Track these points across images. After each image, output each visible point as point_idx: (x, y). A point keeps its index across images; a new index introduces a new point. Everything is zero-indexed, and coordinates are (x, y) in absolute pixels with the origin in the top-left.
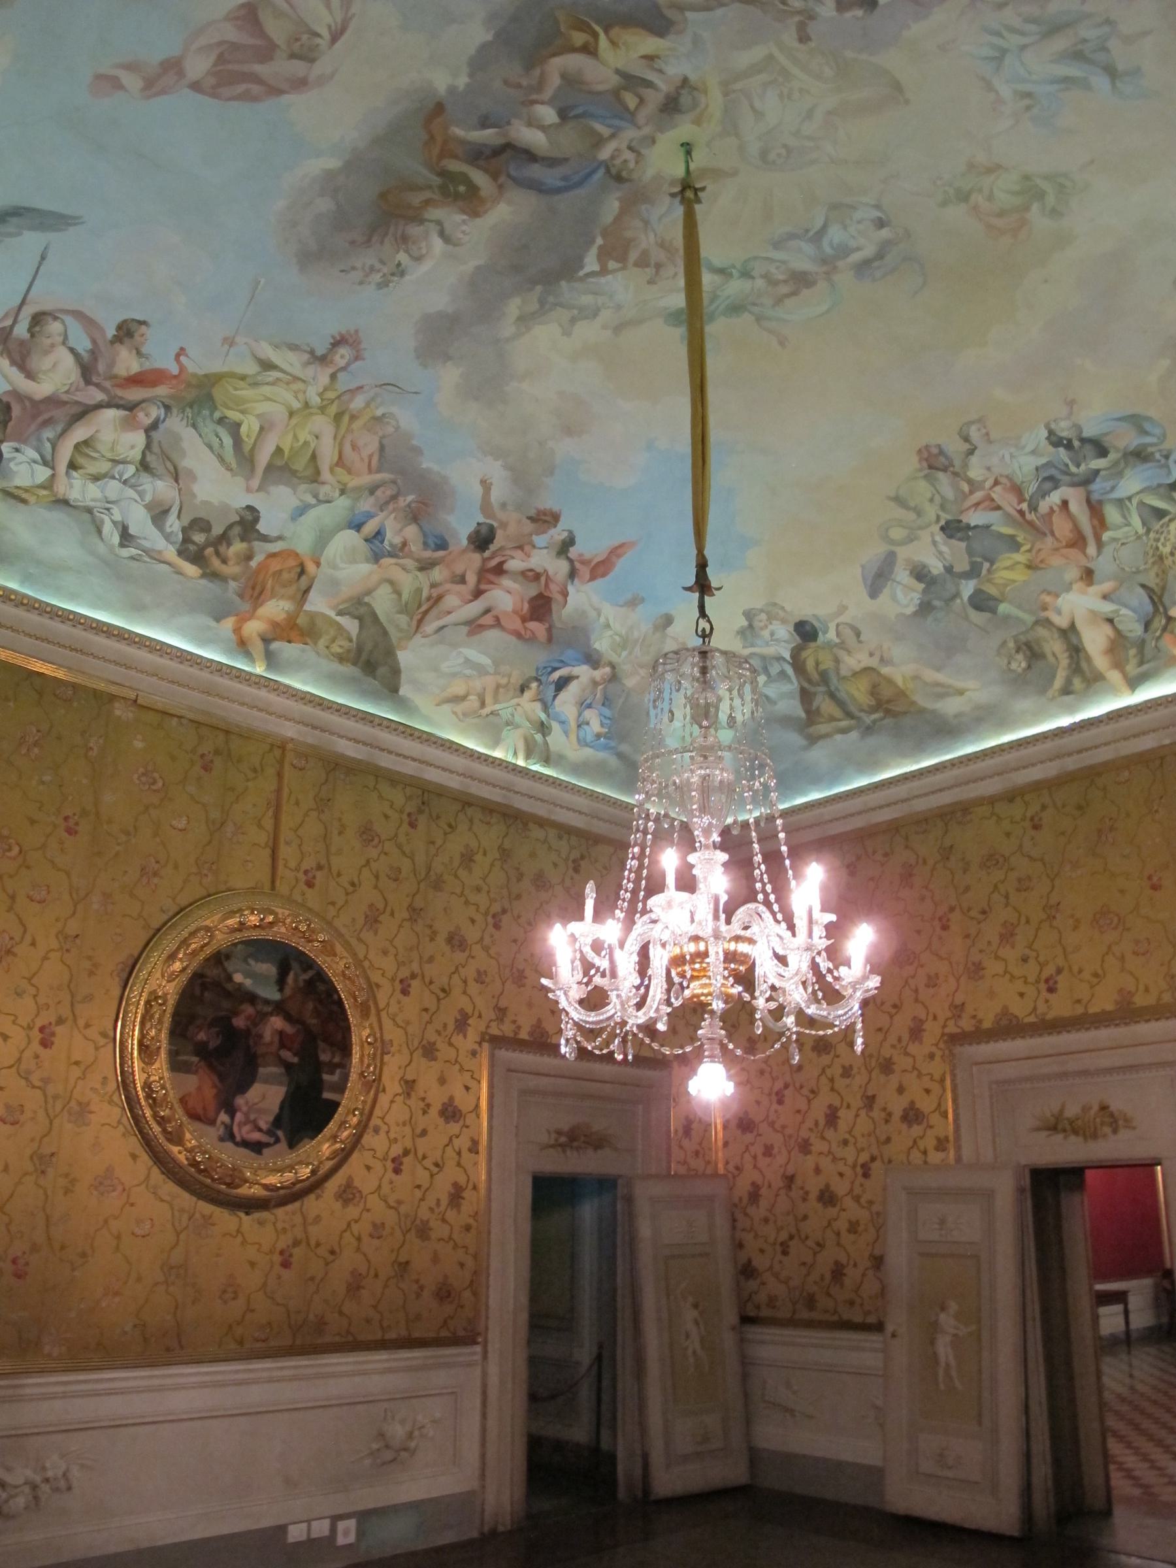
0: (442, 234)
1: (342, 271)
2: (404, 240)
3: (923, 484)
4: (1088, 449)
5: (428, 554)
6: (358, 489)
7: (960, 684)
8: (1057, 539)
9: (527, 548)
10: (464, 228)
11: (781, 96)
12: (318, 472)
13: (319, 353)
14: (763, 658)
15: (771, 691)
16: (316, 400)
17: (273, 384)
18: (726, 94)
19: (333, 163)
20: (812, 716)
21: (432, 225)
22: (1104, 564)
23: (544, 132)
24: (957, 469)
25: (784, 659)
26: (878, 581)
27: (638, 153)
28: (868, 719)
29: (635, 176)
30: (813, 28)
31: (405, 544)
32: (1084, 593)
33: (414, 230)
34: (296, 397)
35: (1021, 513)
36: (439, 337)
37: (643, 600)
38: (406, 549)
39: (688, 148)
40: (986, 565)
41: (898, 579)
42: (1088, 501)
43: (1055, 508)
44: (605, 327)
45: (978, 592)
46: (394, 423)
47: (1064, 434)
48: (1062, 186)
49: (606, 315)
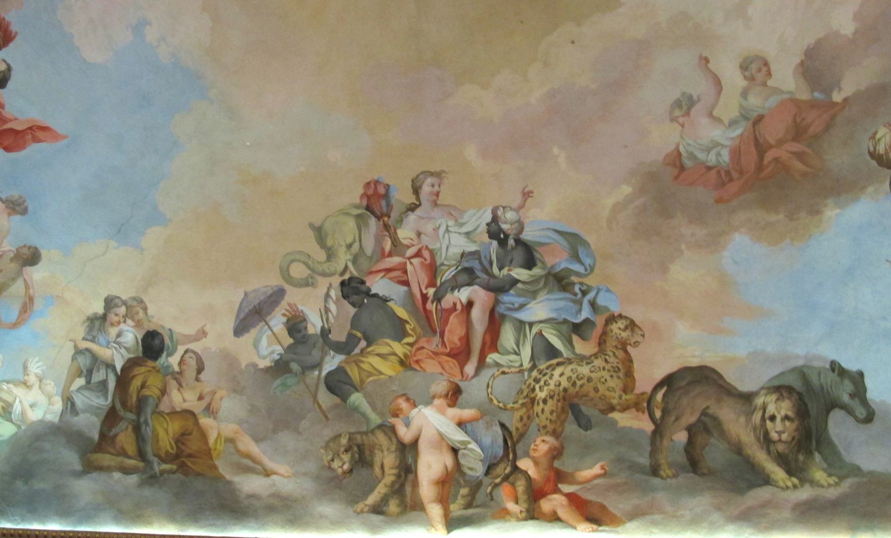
3: (351, 224)
4: (519, 255)
7: (270, 465)
8: (443, 343)
14: (95, 358)
15: (80, 400)
20: (105, 441)
22: (475, 389)
24: (391, 222)
25: (114, 368)
26: (251, 317)
28: (158, 467)
32: (442, 412)
35: (425, 297)
37: (24, 212)
40: (363, 343)
41: (271, 323)
42: (492, 312)
43: (459, 307)
45: (340, 370)
47: (505, 227)
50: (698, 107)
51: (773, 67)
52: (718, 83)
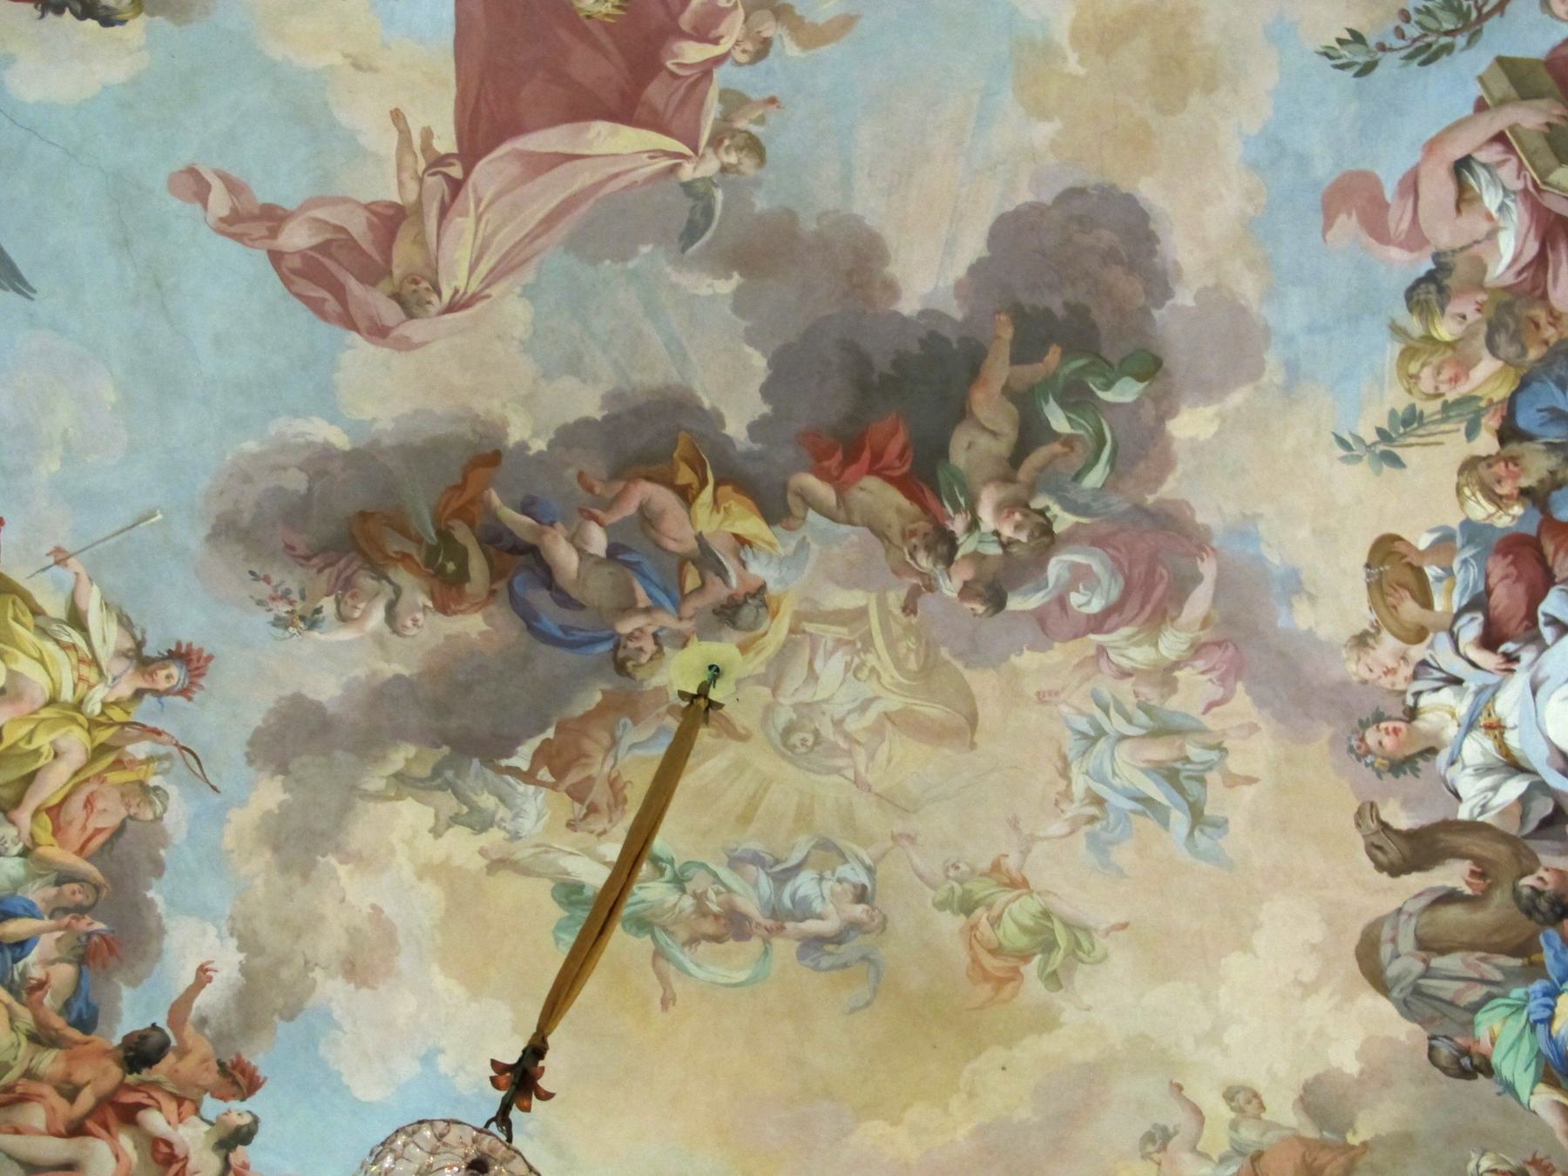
0: (391, 609)
1: (252, 573)
2: (345, 587)
5: (58, 1022)
6: (43, 862)
9: (187, 1105)
10: (419, 616)
11: (848, 666)
12: (17, 802)
13: (150, 650)
16: (94, 707)
17: (64, 647)
18: (792, 631)
19: (340, 440)
21: (388, 589)
23: (581, 559)
27: (660, 650)
29: (639, 674)
30: (926, 602)
31: (42, 985)
33: (366, 582)
34: (75, 686)
36: (293, 736)
38: (39, 993)
39: (715, 672)
44: (483, 852)
46: (159, 808)
48: (1078, 944)
49: (495, 836)
50: (1176, 1139)
51: (1266, 1098)
52: (1197, 1112)
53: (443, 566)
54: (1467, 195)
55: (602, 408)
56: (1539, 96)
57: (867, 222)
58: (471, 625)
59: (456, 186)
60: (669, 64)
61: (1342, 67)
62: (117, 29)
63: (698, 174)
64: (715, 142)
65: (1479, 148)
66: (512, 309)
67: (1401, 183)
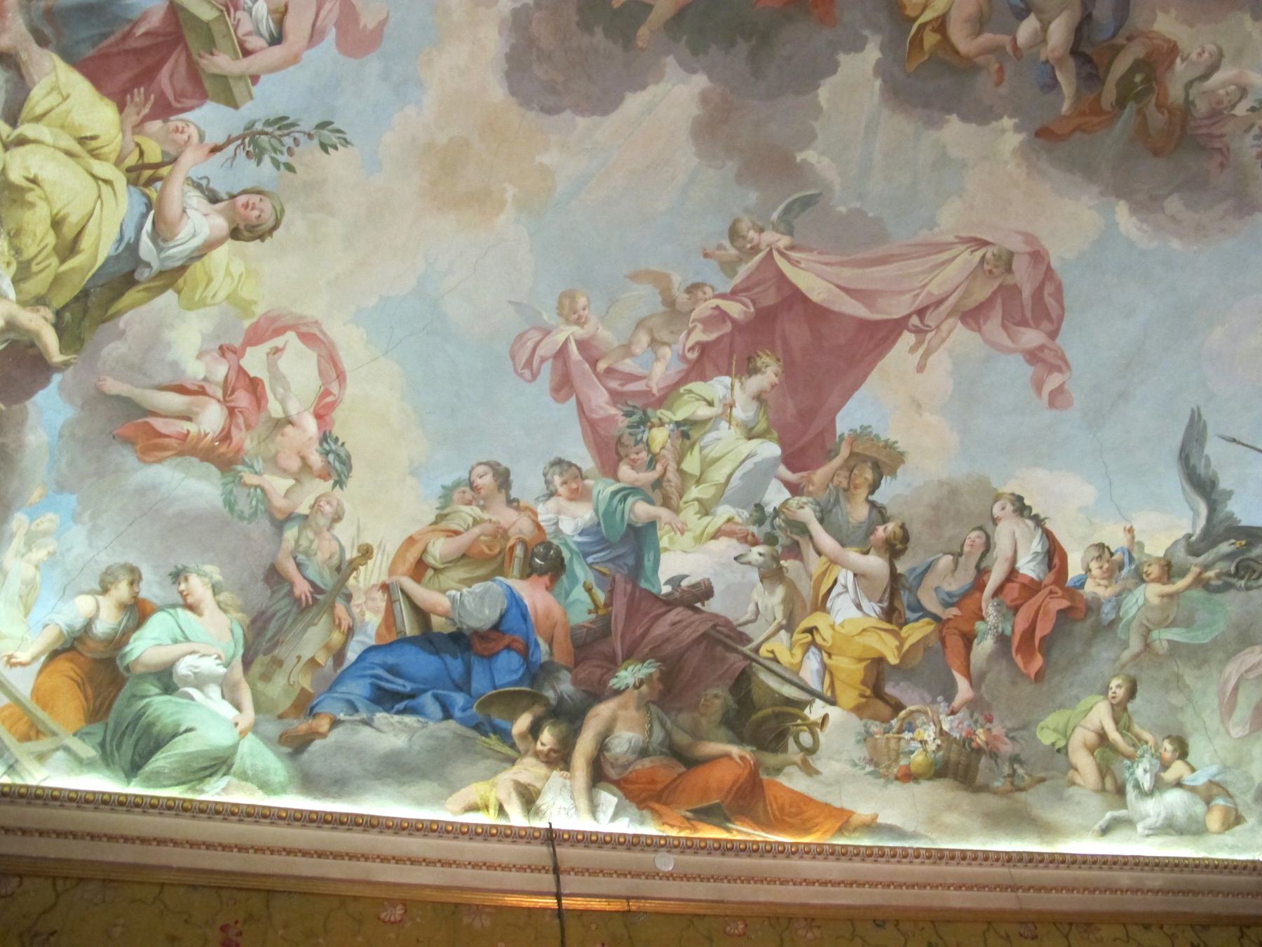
0: (1206, 76)
2: (1218, 114)
10: (1194, 56)
19: (1122, 212)
21: (1193, 92)
23: (1049, 23)
33: (1202, 107)
53: (1142, 82)
54: (278, 16)
55: (947, 121)
56: (215, 76)
57: (694, 150)
58: (1166, 25)
59: (921, 313)
60: (752, 310)
61: (339, 131)
62: (1018, 493)
63: (778, 236)
64: (755, 250)
65: (262, 49)
66: (950, 220)
67: (322, 39)
